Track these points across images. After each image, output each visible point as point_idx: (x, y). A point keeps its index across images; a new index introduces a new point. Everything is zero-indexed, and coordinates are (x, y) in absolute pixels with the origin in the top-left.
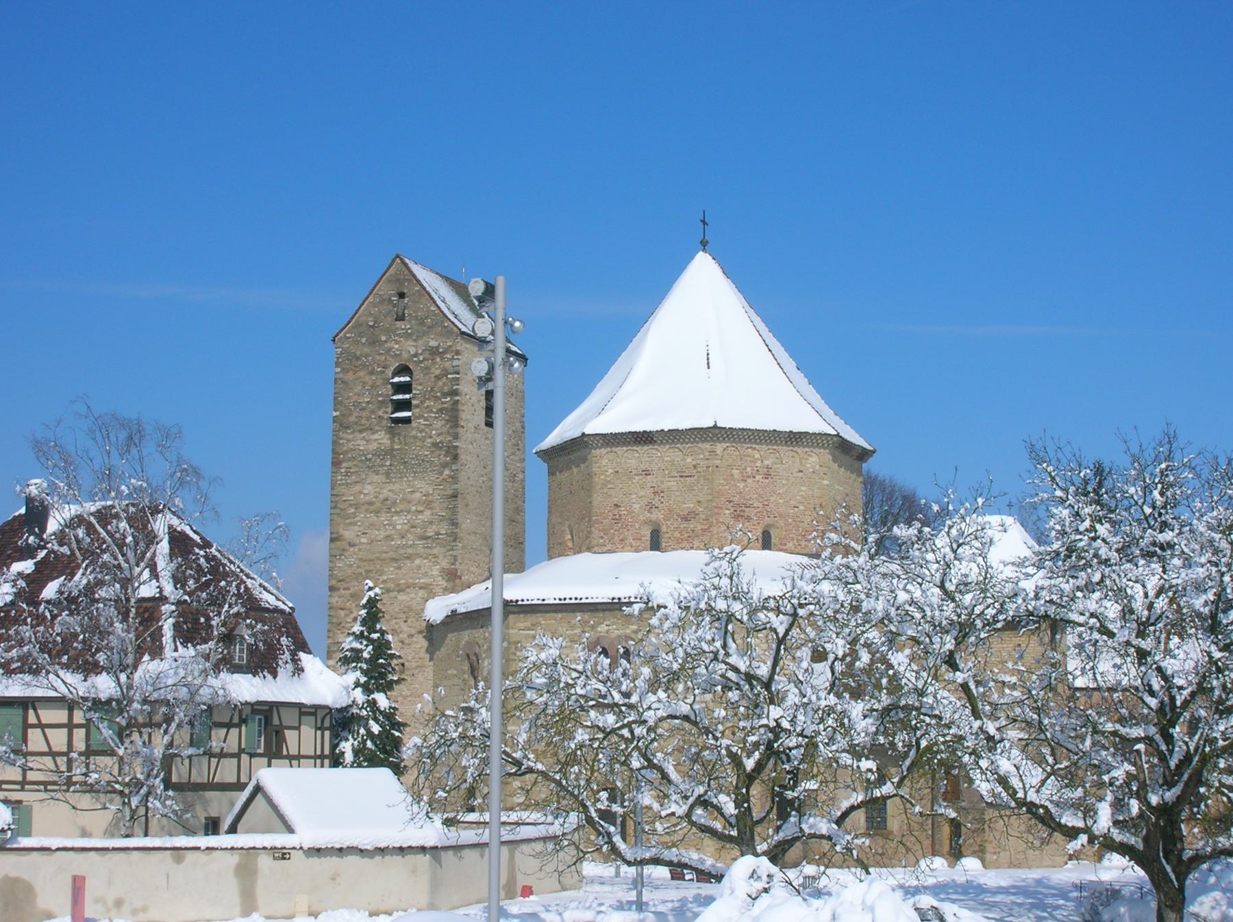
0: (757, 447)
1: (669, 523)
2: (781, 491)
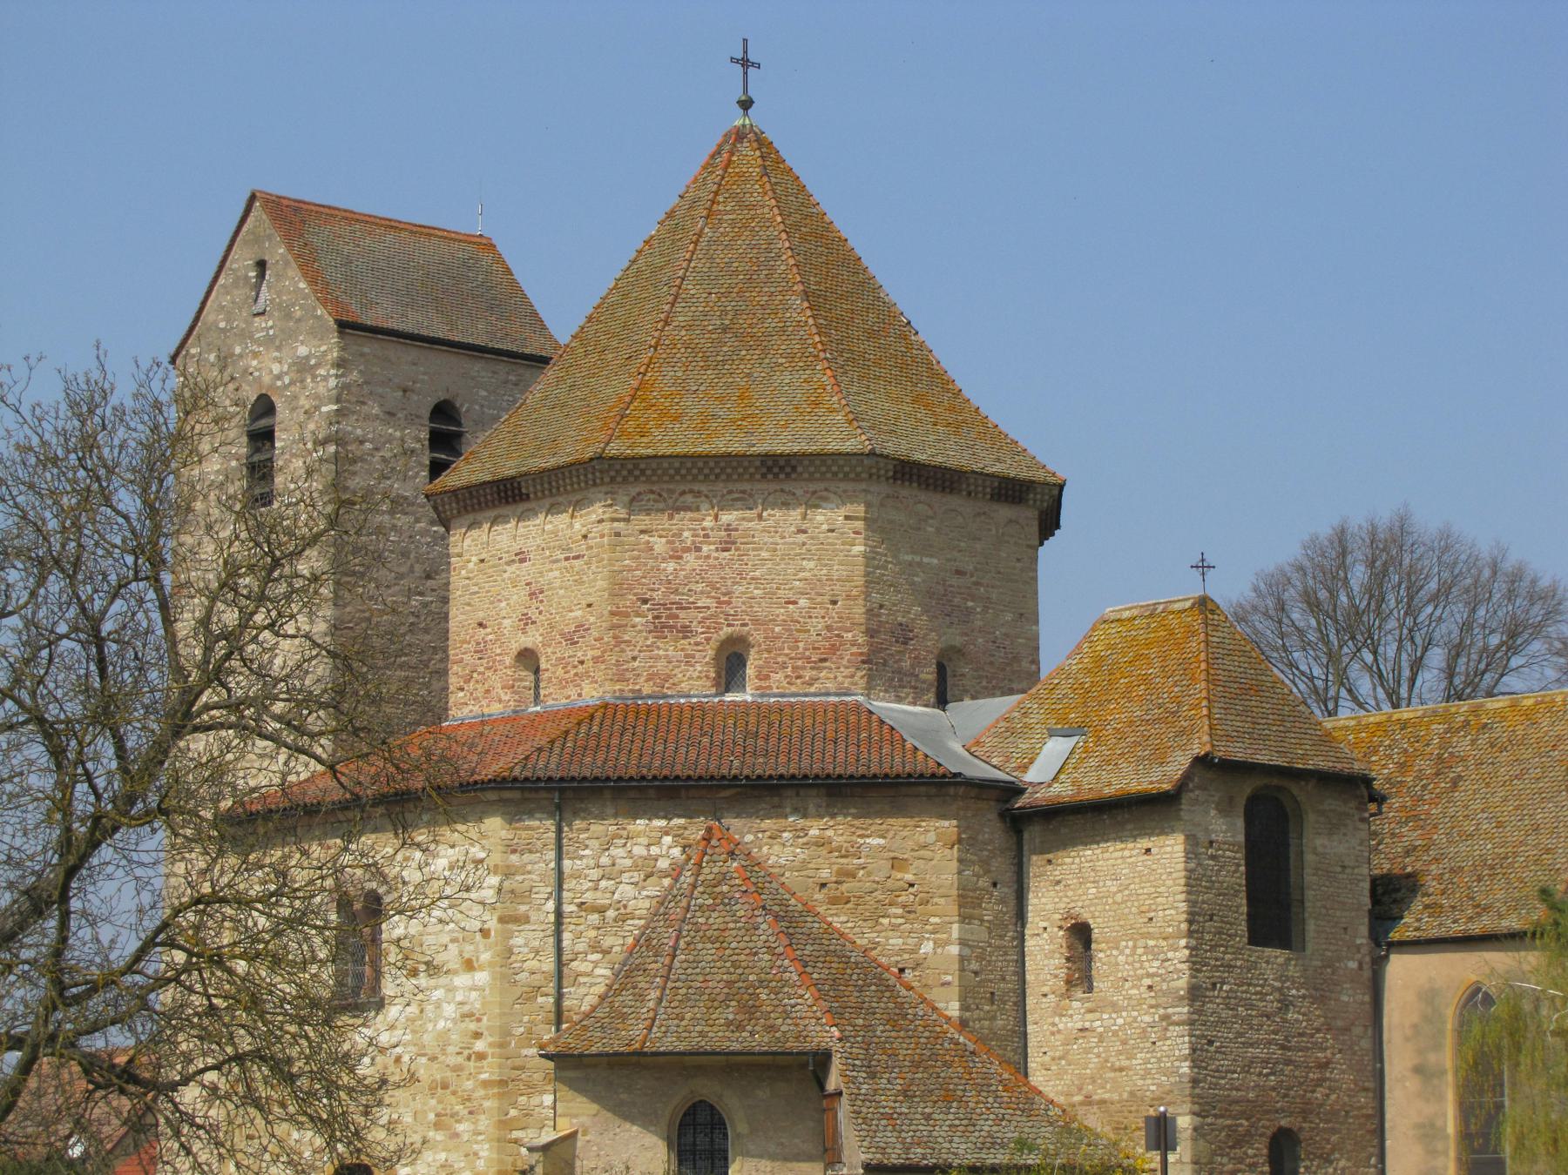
0: (704, 488)
1: (549, 650)
2: (757, 573)
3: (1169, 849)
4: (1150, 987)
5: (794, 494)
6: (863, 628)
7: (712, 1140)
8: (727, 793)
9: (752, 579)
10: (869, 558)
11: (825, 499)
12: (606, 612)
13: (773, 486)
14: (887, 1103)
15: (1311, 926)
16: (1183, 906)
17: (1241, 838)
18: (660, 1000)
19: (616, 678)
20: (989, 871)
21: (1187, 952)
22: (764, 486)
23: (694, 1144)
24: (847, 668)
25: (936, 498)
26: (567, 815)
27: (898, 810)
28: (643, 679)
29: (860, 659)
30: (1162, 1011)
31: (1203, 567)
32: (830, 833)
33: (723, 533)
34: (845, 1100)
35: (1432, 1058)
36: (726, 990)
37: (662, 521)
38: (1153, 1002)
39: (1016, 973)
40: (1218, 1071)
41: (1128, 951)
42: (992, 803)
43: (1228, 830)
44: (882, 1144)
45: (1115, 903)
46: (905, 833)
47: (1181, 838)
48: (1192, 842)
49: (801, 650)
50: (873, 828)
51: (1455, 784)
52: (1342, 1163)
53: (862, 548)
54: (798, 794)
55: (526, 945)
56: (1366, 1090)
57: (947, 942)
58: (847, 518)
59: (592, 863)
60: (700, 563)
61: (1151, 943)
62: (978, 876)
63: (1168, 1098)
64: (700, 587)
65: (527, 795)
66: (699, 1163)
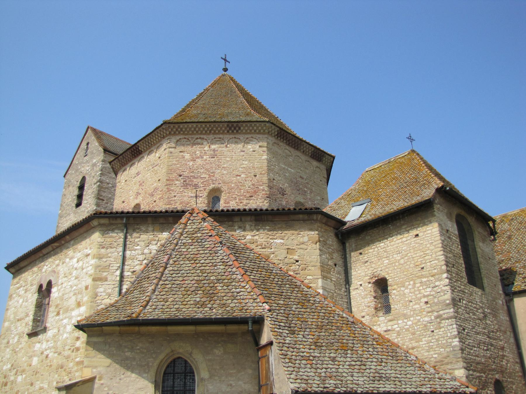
0: (205, 137)
3: (429, 232)
4: (426, 303)
5: (239, 139)
6: (267, 185)
7: (185, 383)
9: (223, 167)
10: (269, 161)
11: (252, 141)
12: (165, 180)
13: (231, 136)
14: (306, 351)
16: (442, 258)
18: (154, 291)
19: (167, 203)
20: (332, 258)
21: (447, 280)
22: (228, 136)
23: (173, 387)
24: (261, 199)
25: (292, 150)
26: (130, 231)
27: (289, 227)
28: (178, 204)
29: (266, 196)
30: (436, 314)
33: (212, 152)
34: (275, 348)
36: (196, 285)
37: (189, 148)
38: (430, 309)
40: (469, 345)
41: (410, 287)
42: (332, 229)
44: (305, 377)
45: (400, 264)
47: (437, 224)
49: (242, 193)
50: (277, 235)
53: (266, 157)
54: (241, 220)
55: (104, 291)
58: (260, 147)
59: (140, 252)
60: (203, 162)
61: (424, 280)
64: (202, 171)
65: (112, 222)
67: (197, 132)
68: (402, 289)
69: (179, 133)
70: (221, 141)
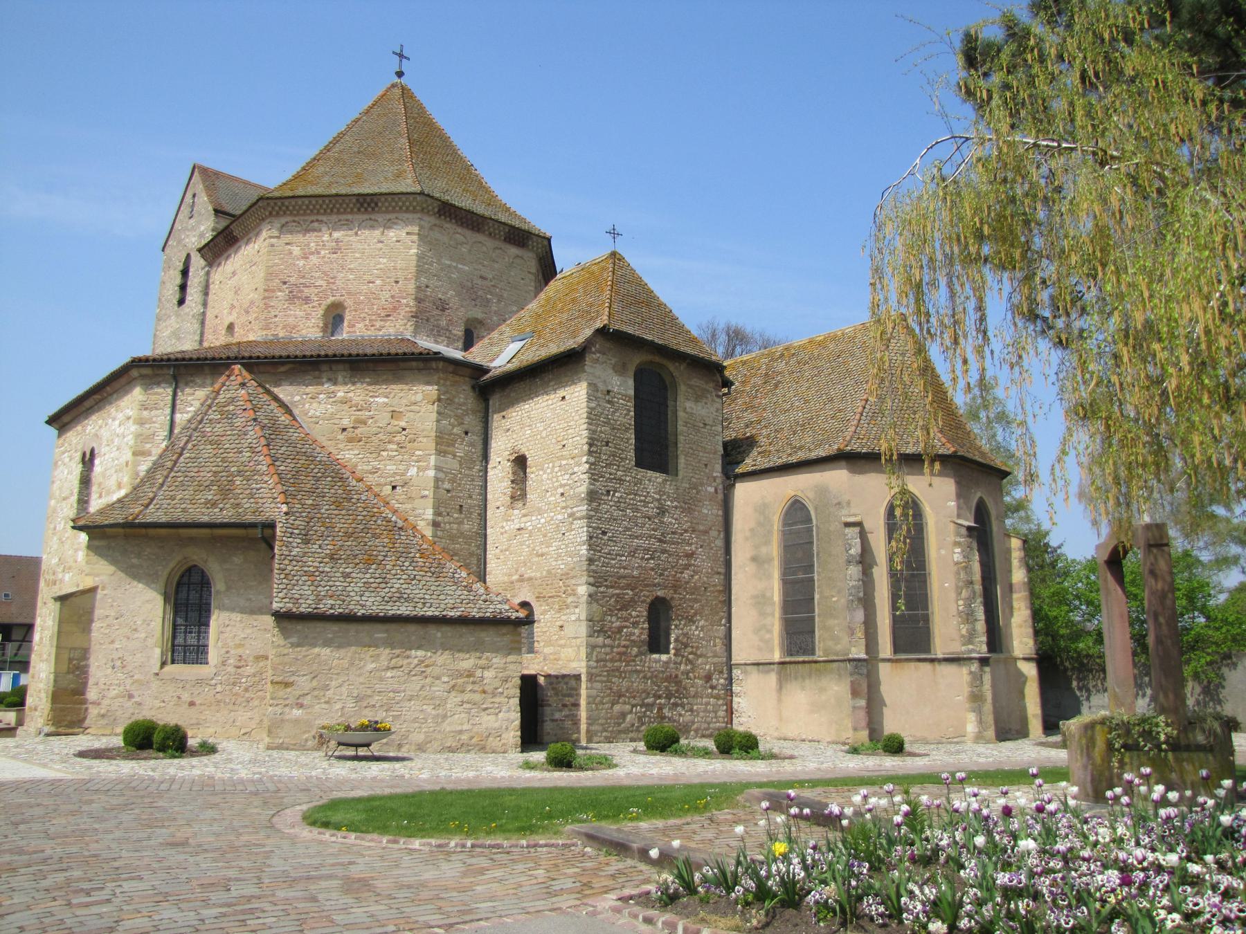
0: (324, 218)
4: (562, 494)
7: (201, 596)
8: (282, 369)
10: (420, 257)
11: (396, 224)
13: (366, 216)
14: (312, 563)
15: (682, 461)
16: (585, 433)
17: (631, 392)
20: (463, 424)
23: (188, 599)
25: (468, 233)
26: (181, 385)
27: (398, 379)
30: (569, 511)
31: (614, 233)
32: (351, 395)
35: (764, 550)
36: (212, 478)
37: (299, 238)
38: (564, 504)
39: (480, 494)
40: (609, 554)
41: (549, 471)
42: (467, 379)
43: (624, 386)
44: (297, 596)
46: (401, 395)
48: (593, 387)
50: (380, 391)
51: (776, 386)
52: (702, 623)
53: (416, 251)
54: (331, 369)
56: (719, 573)
57: (427, 468)
58: (408, 233)
61: (564, 462)
62: (454, 426)
63: (572, 574)
66: (190, 614)
67: (312, 211)
68: (541, 473)
69: (285, 213)
70: (348, 225)
